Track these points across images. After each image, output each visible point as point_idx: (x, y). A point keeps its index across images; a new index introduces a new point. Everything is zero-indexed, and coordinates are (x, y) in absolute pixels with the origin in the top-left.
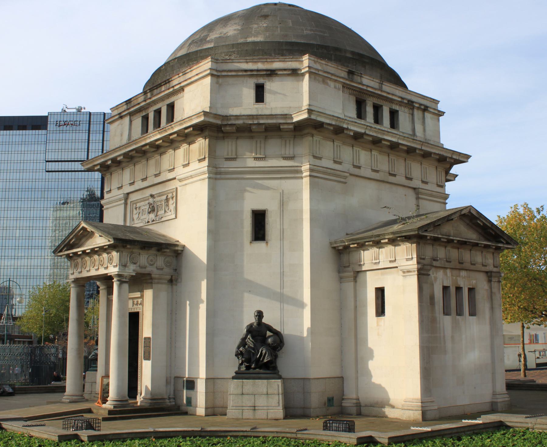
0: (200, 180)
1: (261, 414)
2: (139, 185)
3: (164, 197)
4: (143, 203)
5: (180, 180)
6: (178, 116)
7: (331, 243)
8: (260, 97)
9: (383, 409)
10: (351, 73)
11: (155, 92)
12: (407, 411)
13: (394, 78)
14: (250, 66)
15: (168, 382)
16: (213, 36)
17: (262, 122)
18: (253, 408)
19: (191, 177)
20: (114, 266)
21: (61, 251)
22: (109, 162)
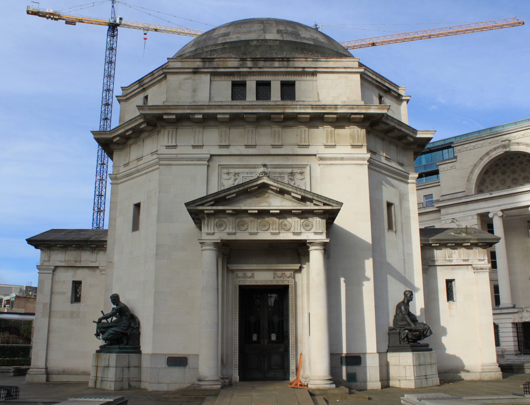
0: (356, 164)
3: (289, 170)
5: (321, 159)
9: (459, 374)
11: (261, 64)
12: (488, 373)
17: (403, 129)
18: (427, 377)
19: (342, 159)
20: (316, 233)
21: (203, 205)
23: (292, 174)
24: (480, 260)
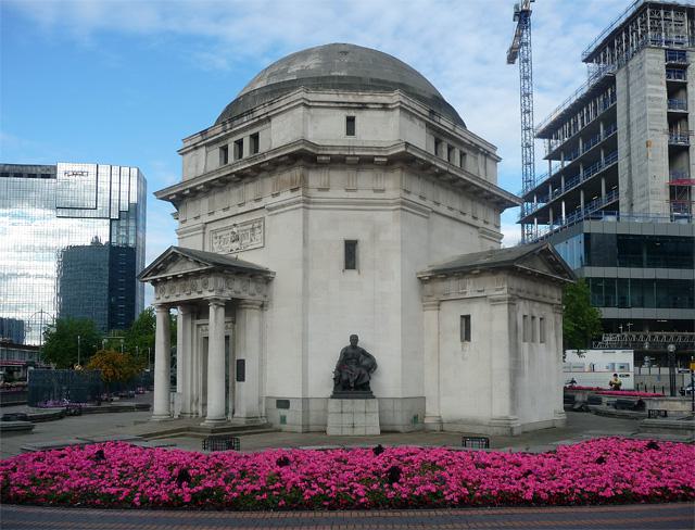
1: (359, 431)
2: (220, 214)
3: (251, 226)
4: (226, 232)
5: (270, 210)
6: (262, 148)
7: (417, 274)
8: (351, 130)
10: (432, 112)
11: (236, 122)
13: (459, 122)
14: (341, 98)
15: (260, 402)
16: (295, 68)
17: (357, 153)
19: (283, 206)
20: (210, 291)
22: (188, 192)
23: (253, 229)
24: (497, 290)
